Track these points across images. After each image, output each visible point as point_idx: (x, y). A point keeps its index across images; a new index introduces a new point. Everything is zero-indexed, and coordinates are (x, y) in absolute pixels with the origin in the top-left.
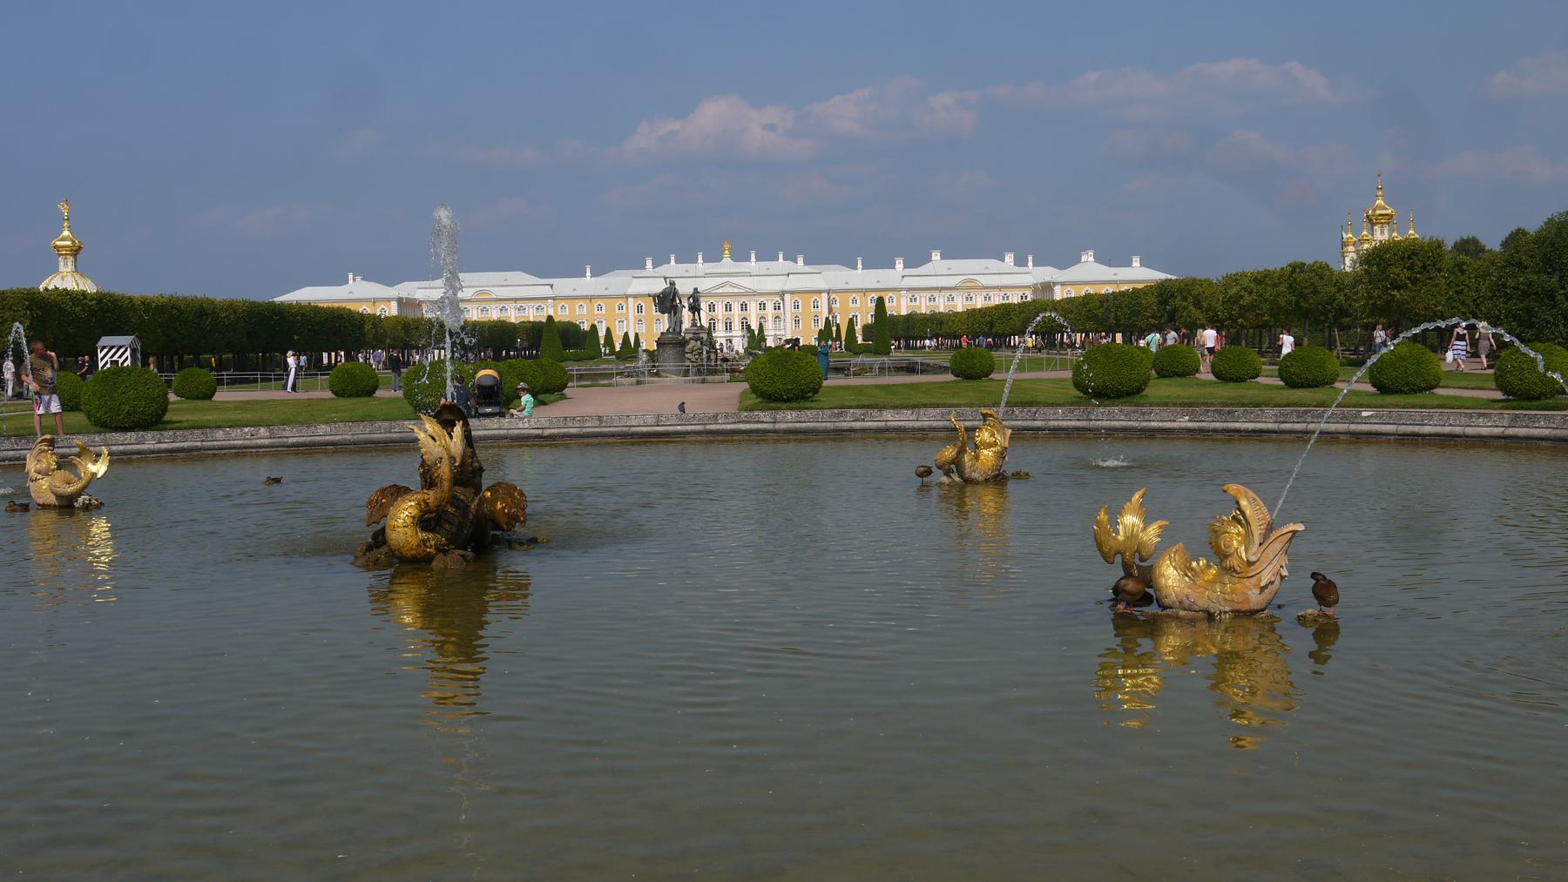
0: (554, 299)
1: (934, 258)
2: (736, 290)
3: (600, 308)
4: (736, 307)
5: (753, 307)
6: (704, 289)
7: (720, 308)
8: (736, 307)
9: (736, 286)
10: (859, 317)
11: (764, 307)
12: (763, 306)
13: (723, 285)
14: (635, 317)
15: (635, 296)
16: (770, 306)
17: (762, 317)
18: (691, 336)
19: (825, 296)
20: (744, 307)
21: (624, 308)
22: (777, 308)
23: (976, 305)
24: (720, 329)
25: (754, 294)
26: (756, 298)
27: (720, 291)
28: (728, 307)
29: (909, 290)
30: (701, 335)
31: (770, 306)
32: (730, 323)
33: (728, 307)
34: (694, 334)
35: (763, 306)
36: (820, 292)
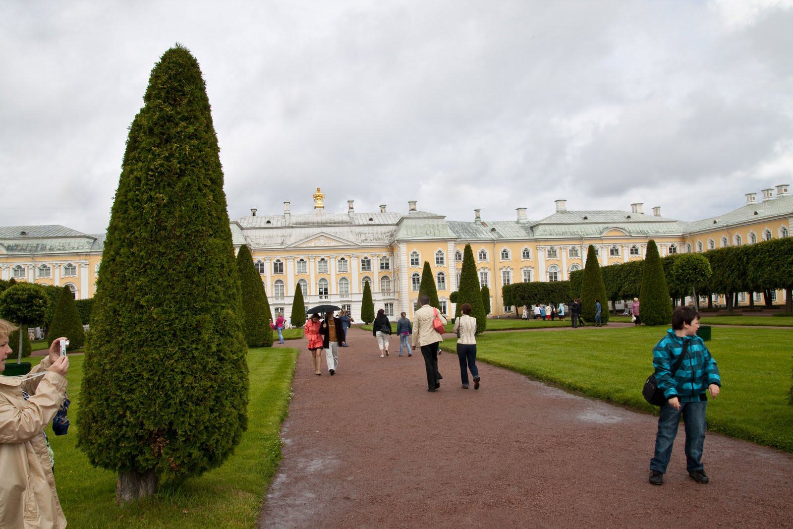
0: (87, 254)
2: (333, 244)
4: (333, 266)
5: (355, 265)
6: (290, 243)
7: (312, 267)
8: (333, 266)
10: (489, 275)
11: (369, 265)
12: (366, 264)
16: (375, 264)
23: (623, 259)
24: (313, 293)
26: (357, 253)
27: (312, 244)
31: (375, 264)
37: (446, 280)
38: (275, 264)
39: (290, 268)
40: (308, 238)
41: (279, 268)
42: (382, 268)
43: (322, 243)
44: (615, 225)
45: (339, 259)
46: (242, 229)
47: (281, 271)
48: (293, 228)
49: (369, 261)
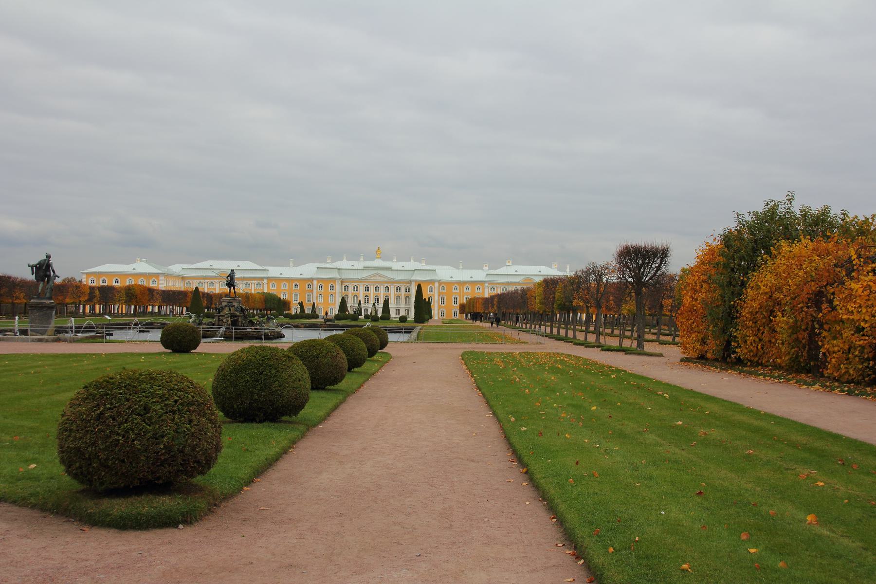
1: (507, 264)
3: (296, 286)
4: (382, 289)
5: (393, 290)
8: (382, 289)
9: (380, 276)
10: (458, 299)
12: (398, 289)
13: (374, 275)
14: (317, 292)
15: (318, 280)
16: (403, 289)
17: (398, 296)
18: (226, 304)
19: (437, 284)
20: (387, 289)
21: (311, 286)
22: (408, 290)
25: (393, 282)
28: (377, 289)
29: (490, 283)
30: (234, 304)
31: (403, 289)
32: (378, 299)
33: (377, 289)
34: (228, 302)
35: (398, 289)
36: (433, 282)
37: (433, 300)
38: (354, 287)
39: (361, 289)
40: (371, 276)
41: (356, 289)
42: (406, 291)
43: (378, 278)
44: (525, 277)
45: (385, 286)
46: (339, 269)
47: (357, 290)
48: (363, 270)
49: (400, 288)
